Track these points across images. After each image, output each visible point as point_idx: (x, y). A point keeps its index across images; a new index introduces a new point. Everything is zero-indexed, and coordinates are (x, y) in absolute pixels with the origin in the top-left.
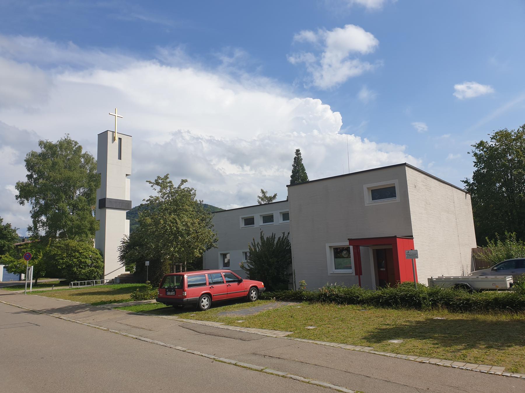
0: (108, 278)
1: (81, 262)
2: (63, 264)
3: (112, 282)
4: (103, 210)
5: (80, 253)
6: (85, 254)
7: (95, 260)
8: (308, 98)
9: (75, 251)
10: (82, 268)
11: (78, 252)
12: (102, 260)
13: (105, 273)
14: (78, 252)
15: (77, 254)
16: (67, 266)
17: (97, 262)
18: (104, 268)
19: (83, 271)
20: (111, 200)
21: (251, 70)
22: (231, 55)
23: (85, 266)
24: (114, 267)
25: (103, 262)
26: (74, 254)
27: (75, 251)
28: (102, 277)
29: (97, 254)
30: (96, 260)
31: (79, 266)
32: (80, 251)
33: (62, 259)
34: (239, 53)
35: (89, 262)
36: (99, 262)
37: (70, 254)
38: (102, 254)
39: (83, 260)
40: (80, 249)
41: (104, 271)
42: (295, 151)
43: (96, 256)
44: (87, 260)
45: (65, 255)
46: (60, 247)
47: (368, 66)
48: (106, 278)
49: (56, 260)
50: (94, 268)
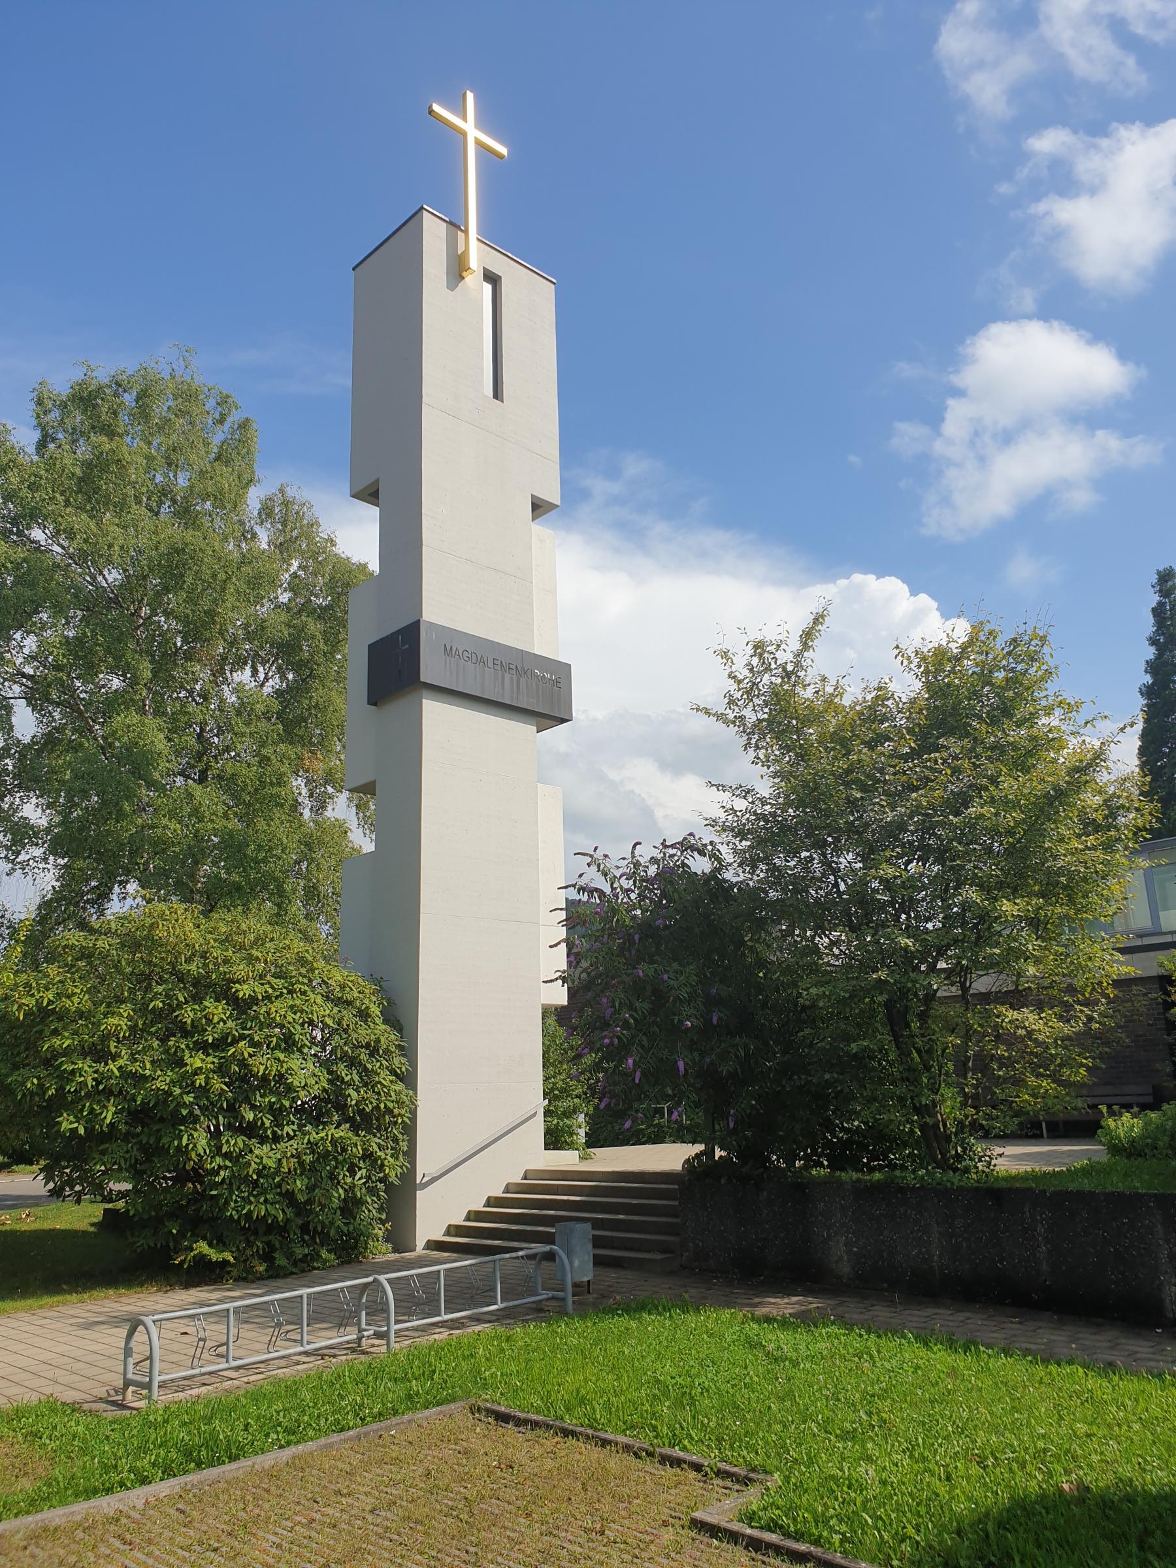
0: (436, 1213)
1: (244, 1082)
2: (102, 1092)
3: (451, 1245)
4: (395, 709)
5: (241, 1006)
6: (278, 1009)
7: (353, 1062)
8: (858, 578)
9: (200, 988)
10: (250, 1131)
11: (225, 993)
12: (398, 1061)
13: (424, 1167)
14: (225, 993)
15: (217, 1009)
16: (139, 1115)
17: (368, 1080)
18: (410, 1130)
19: (265, 1155)
20: (459, 646)
21: (674, 510)
22: (613, 473)
23: (278, 1114)
24: (482, 1117)
25: (408, 1078)
26: (188, 1015)
27: (200, 988)
28: (399, 1198)
29: (364, 1015)
30: (349, 1057)
31: (232, 1109)
32: (244, 991)
33: (100, 1053)
34: (635, 466)
35: (306, 1075)
36: (385, 1077)
37: (158, 1015)
38: (400, 1017)
39: (261, 1064)
40: (240, 969)
41: (411, 1154)
42: (1154, 579)
43: (363, 1034)
44: (294, 1062)
45: (119, 1021)
46: (86, 954)
47: (1110, 442)
48: (423, 1199)
49: (48, 1062)
50: (343, 1132)
